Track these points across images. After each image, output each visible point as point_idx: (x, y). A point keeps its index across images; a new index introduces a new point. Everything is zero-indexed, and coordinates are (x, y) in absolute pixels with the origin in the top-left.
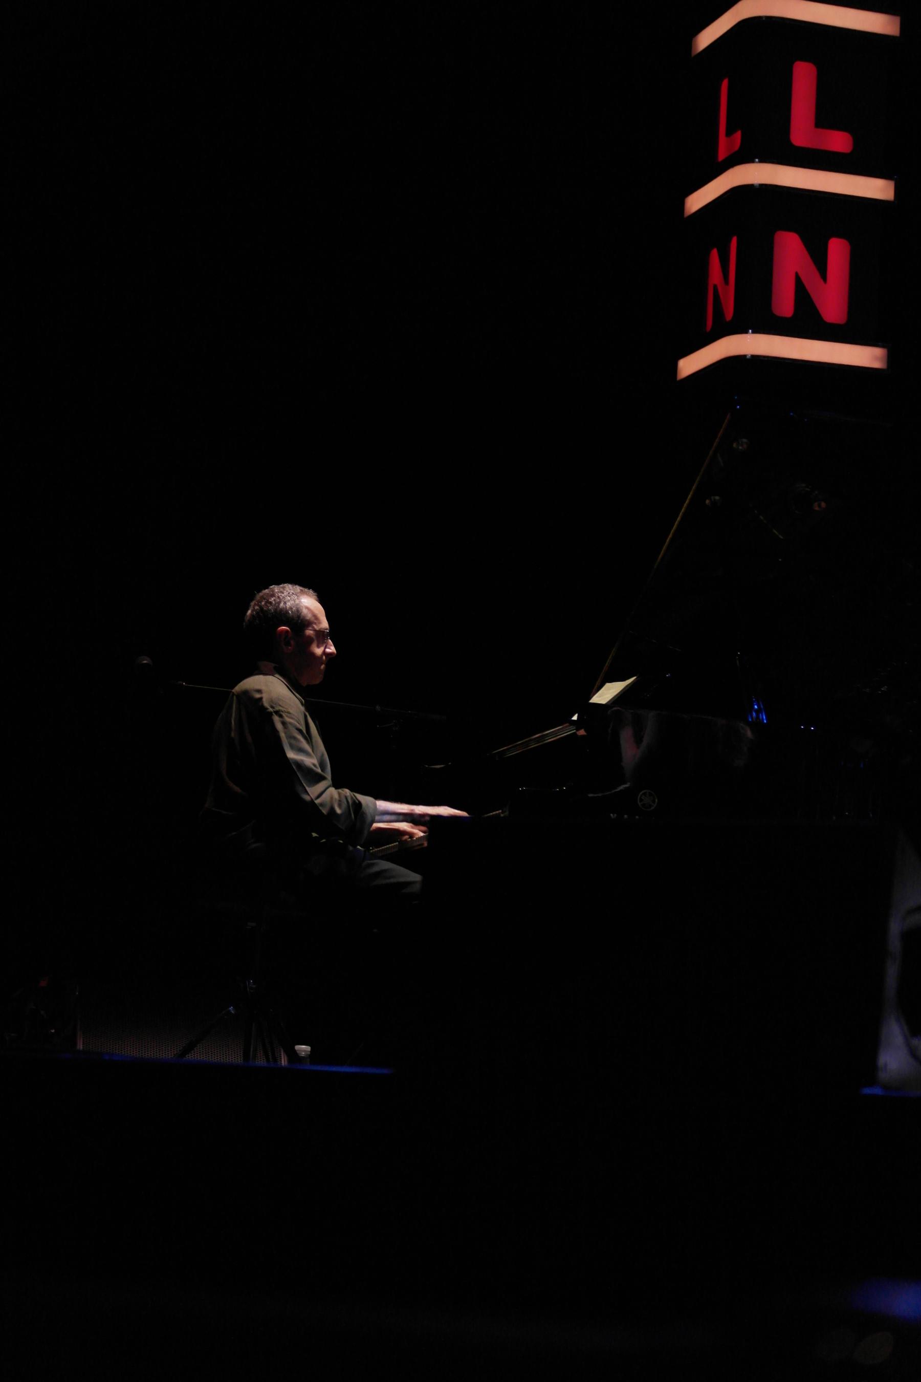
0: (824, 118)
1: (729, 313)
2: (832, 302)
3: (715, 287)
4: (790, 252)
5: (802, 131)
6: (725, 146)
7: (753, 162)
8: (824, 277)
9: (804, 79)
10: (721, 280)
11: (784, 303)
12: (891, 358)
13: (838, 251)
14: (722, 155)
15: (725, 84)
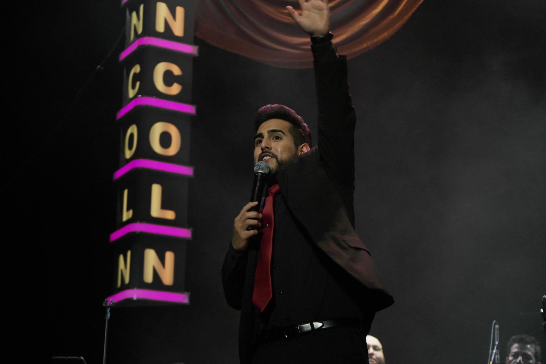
0: (164, 206)
1: (127, 280)
2: (167, 277)
4: (151, 256)
5: (156, 211)
6: (127, 215)
9: (156, 190)
10: (124, 267)
11: (149, 278)
12: (191, 299)
13: (169, 256)
15: (126, 192)
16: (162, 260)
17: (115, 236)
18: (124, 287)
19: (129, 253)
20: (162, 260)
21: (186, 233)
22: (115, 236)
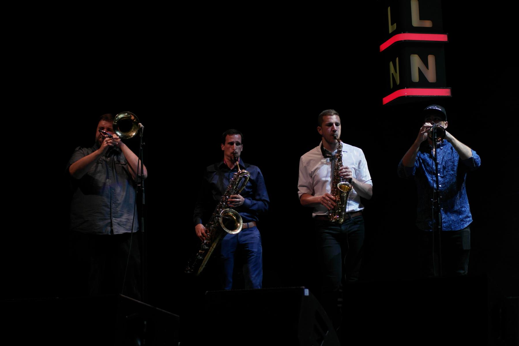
0: (422, 17)
1: (398, 82)
2: (431, 75)
3: (392, 74)
4: (416, 61)
5: (416, 21)
6: (391, 28)
7: (401, 33)
8: (427, 67)
10: (394, 71)
11: (415, 77)
12: (452, 92)
13: (431, 59)
14: (390, 31)
15: (389, 8)
16: (426, 63)
17: (384, 47)
18: (397, 88)
19: (397, 59)
20: (426, 63)
21: (443, 38)
22: (384, 47)
